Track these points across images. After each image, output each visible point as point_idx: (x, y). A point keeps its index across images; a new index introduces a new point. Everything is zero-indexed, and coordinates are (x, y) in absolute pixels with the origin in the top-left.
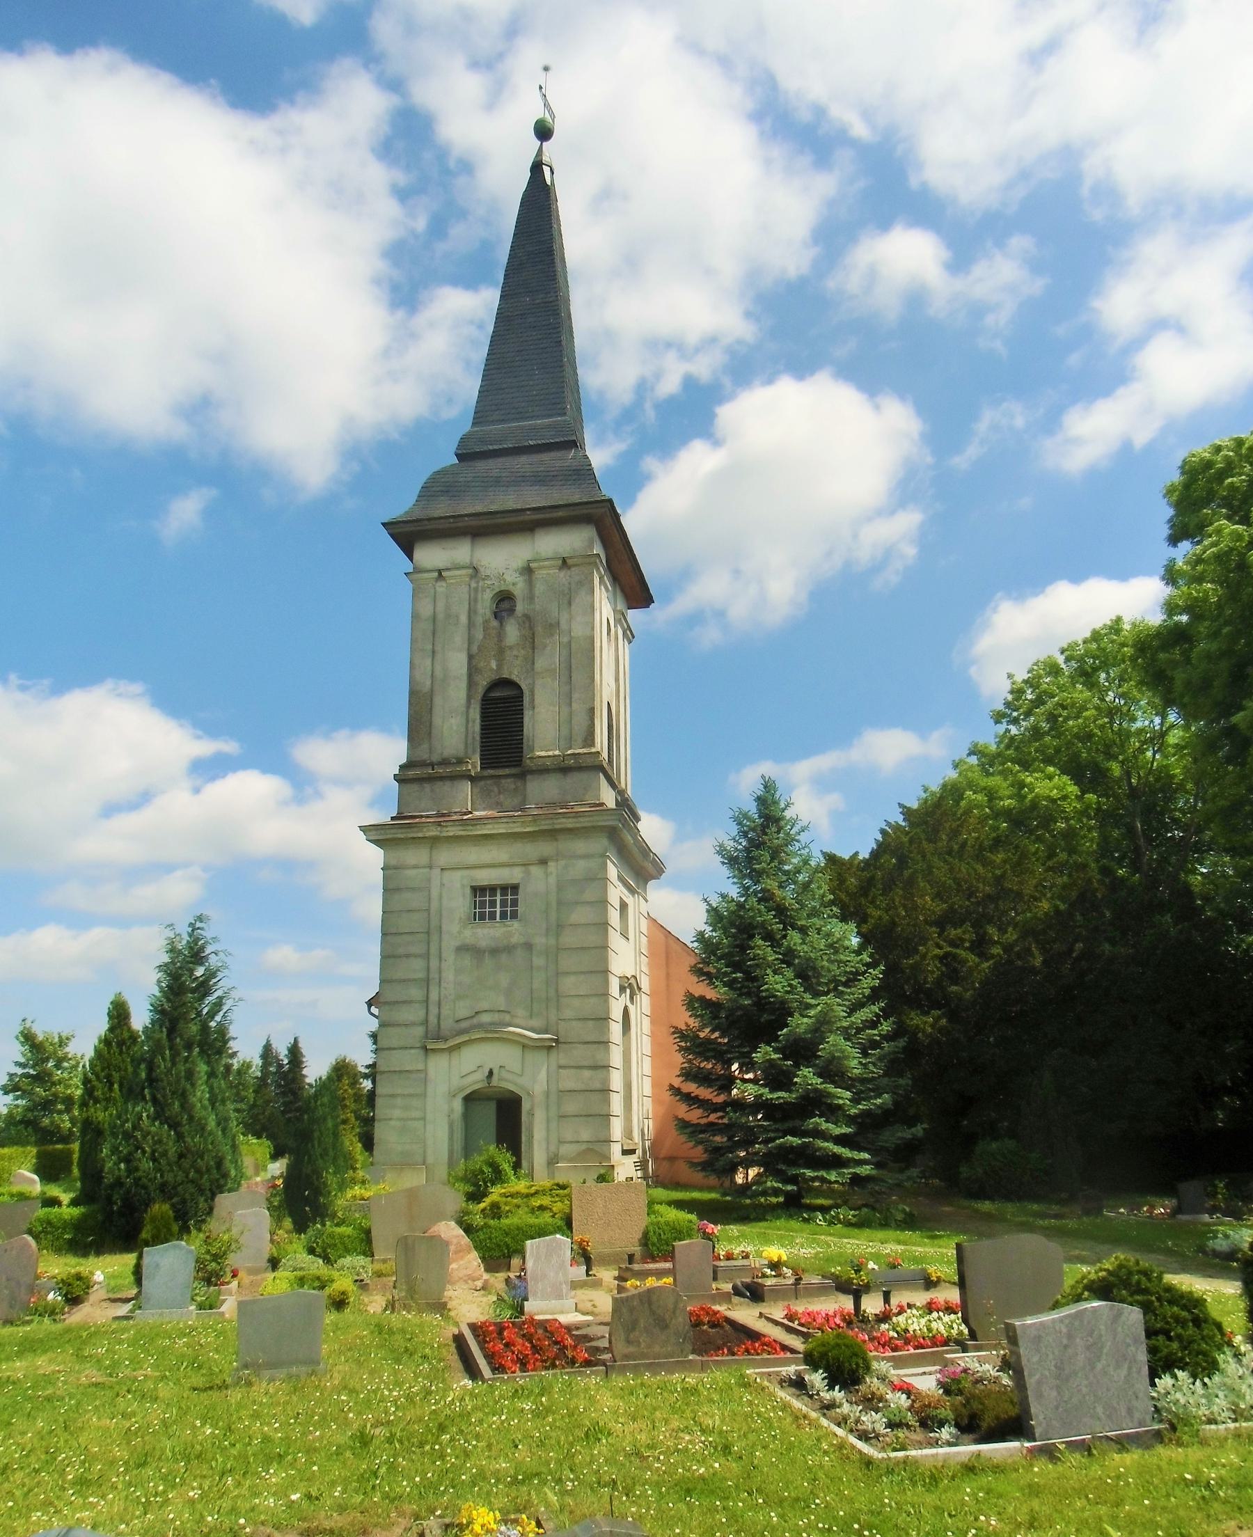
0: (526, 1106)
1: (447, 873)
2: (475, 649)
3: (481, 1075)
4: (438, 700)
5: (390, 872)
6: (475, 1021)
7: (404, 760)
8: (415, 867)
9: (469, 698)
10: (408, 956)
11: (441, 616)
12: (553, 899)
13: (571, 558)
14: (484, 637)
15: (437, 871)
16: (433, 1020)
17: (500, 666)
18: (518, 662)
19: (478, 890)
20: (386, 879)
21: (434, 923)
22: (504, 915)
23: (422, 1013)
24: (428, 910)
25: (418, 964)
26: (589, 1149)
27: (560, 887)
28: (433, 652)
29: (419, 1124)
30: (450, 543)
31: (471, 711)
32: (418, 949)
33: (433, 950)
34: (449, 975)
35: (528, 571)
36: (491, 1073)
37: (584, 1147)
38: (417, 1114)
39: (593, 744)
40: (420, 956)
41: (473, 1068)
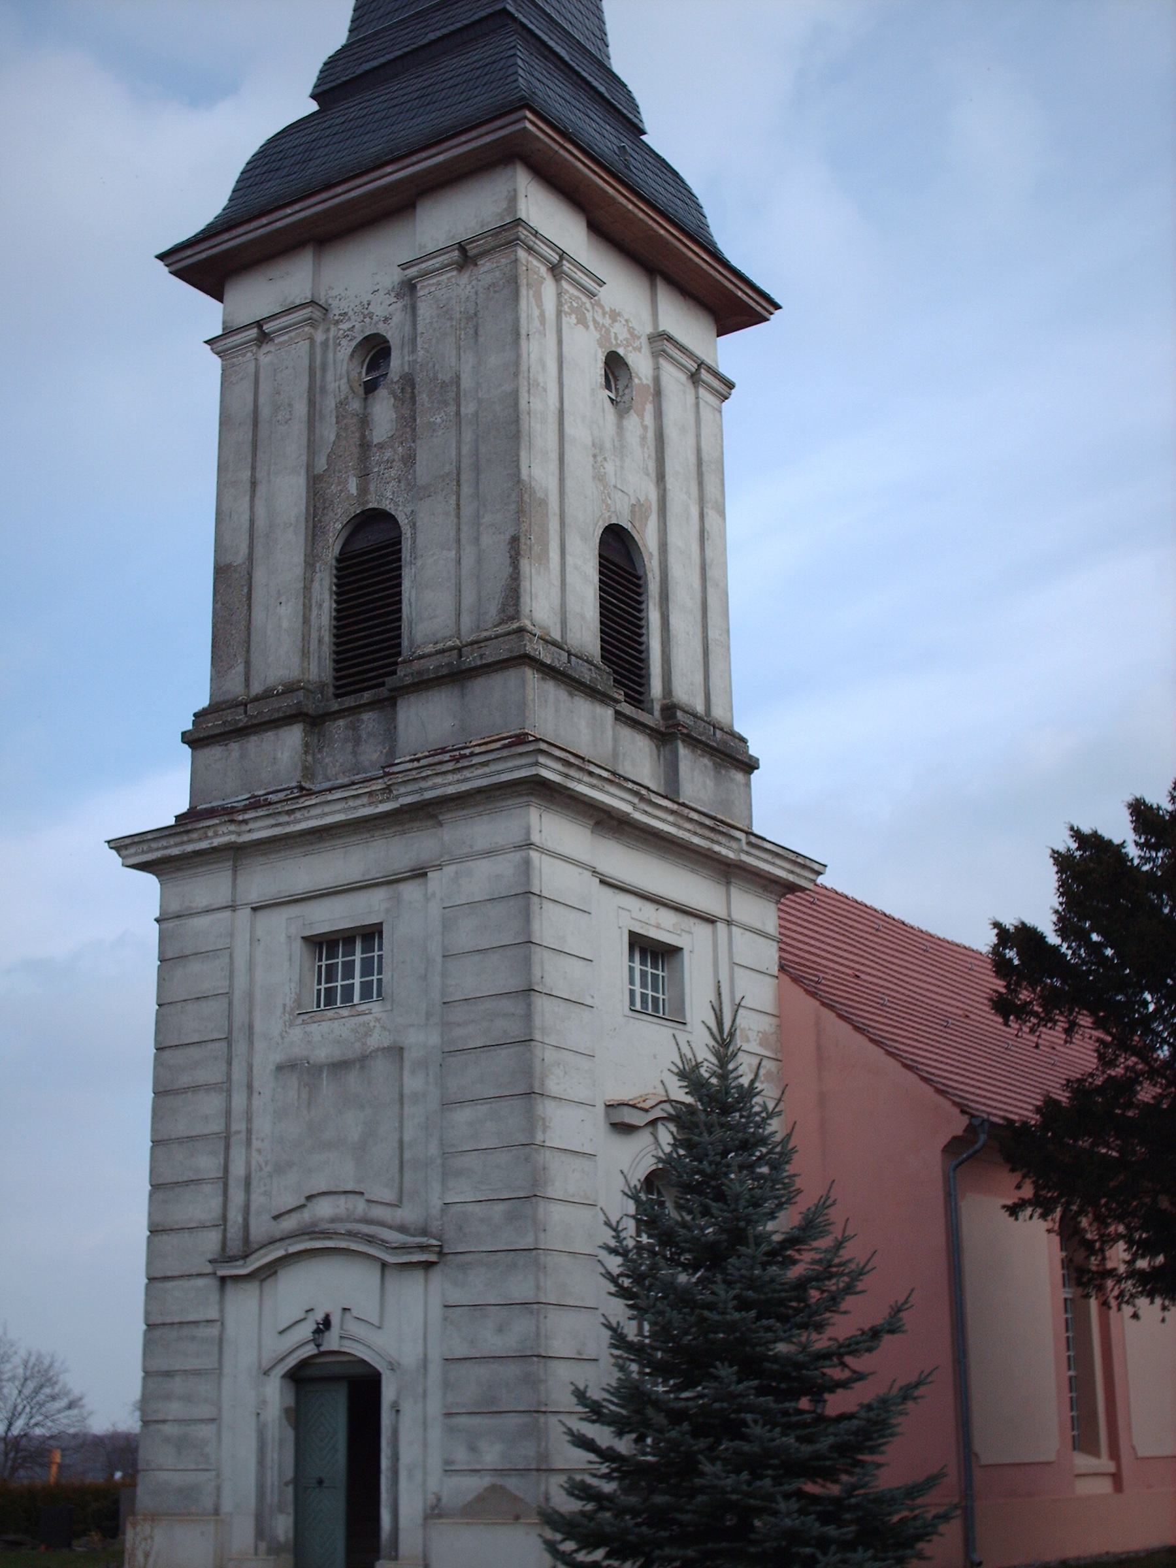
0: (388, 1394)
1: (261, 915)
2: (321, 464)
3: (305, 1331)
4: (259, 575)
5: (170, 925)
6: (306, 1216)
7: (204, 702)
8: (208, 911)
9: (310, 563)
10: (195, 1088)
11: (265, 412)
12: (435, 949)
13: (472, 240)
14: (338, 436)
15: (244, 914)
16: (235, 1217)
17: (363, 490)
18: (393, 472)
21: (239, 1018)
22: (366, 993)
23: (216, 1203)
24: (228, 995)
25: (212, 1104)
26: (493, 1489)
27: (447, 925)
28: (254, 484)
29: (206, 1431)
30: (278, 269)
31: (316, 585)
32: (212, 1074)
33: (238, 1074)
34: (263, 1125)
35: (409, 288)
36: (327, 1323)
37: (486, 1481)
38: (206, 1411)
39: (516, 616)
40: (208, 1088)
41: (300, 1315)
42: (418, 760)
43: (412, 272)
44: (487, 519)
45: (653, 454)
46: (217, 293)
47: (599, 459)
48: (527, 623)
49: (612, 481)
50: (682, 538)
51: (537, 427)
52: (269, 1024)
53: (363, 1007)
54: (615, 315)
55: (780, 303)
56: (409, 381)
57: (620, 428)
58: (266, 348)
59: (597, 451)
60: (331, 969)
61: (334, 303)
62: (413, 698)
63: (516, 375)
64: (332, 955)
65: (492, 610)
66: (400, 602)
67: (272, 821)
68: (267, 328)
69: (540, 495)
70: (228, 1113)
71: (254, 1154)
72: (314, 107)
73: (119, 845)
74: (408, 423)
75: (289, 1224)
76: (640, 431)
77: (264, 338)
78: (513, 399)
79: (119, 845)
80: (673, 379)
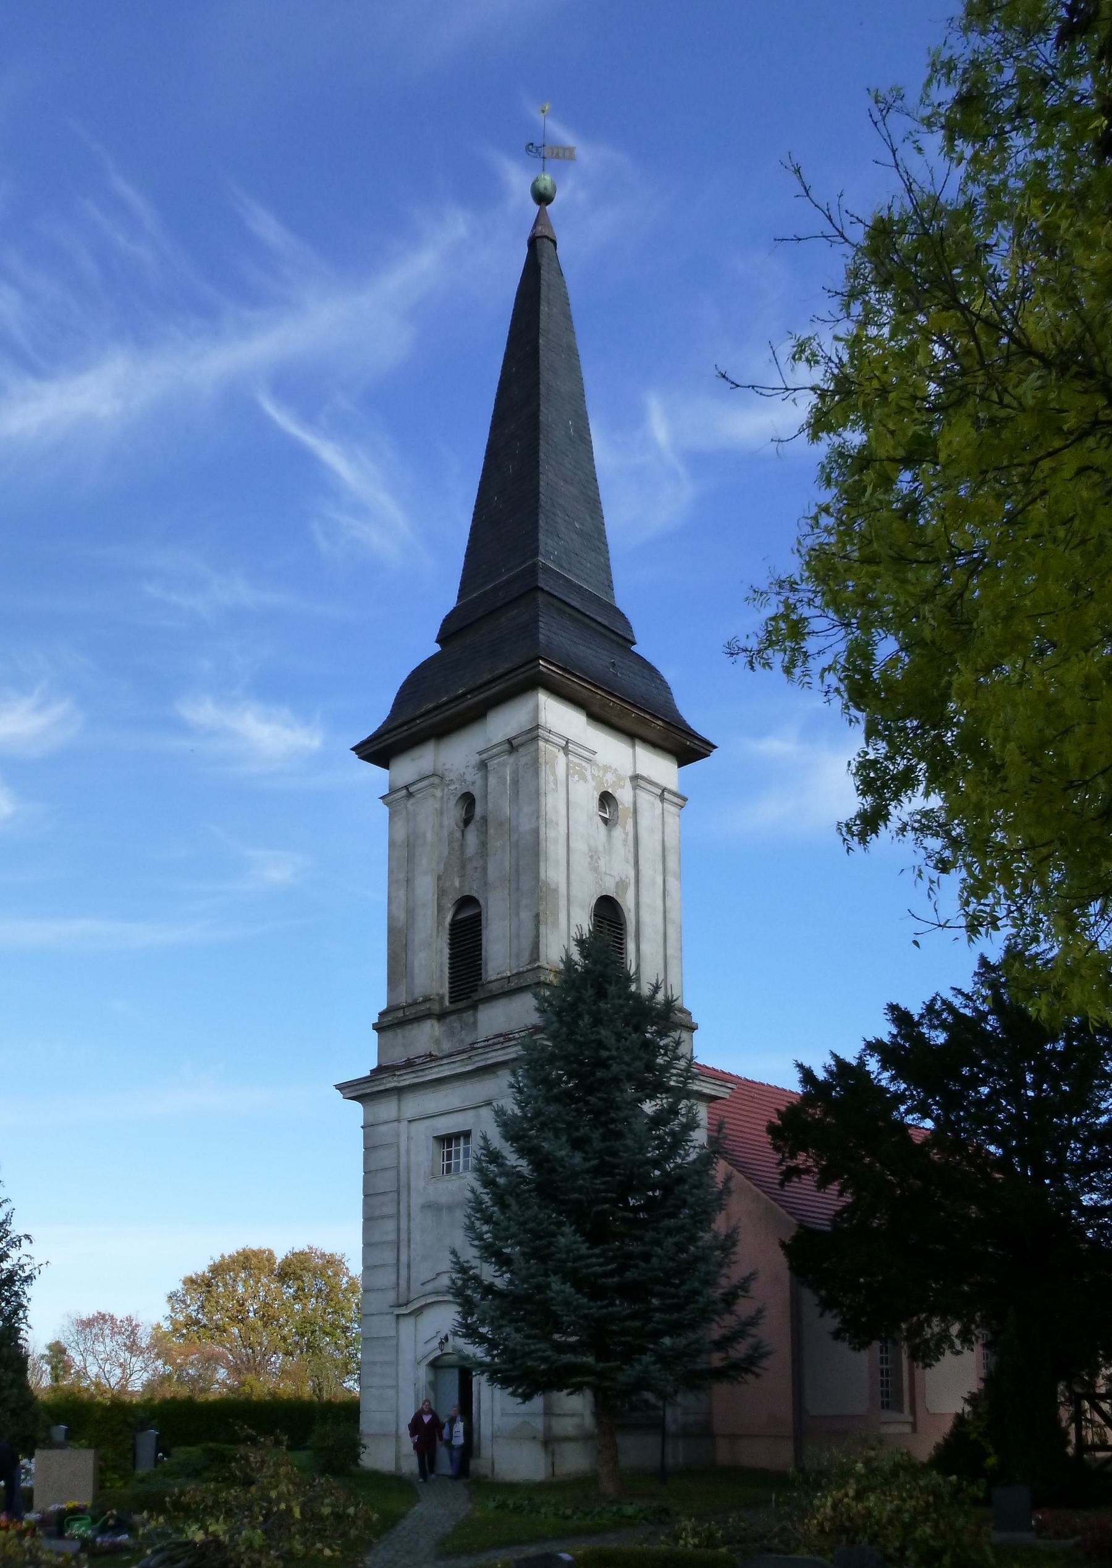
1: (415, 1125)
7: (383, 1006)
10: (383, 1217)
15: (404, 1124)
17: (462, 886)
19: (446, 1140)
20: (366, 1137)
23: (393, 1277)
24: (398, 1167)
30: (417, 752)
32: (390, 1209)
34: (416, 1236)
35: (483, 766)
36: (446, 1339)
39: (537, 959)
42: (488, 1040)
43: (485, 756)
44: (524, 902)
45: (632, 850)
46: (386, 765)
47: (595, 857)
48: (542, 963)
49: (603, 869)
50: (651, 897)
51: (551, 847)
52: (418, 1183)
53: (464, 1174)
54: (606, 768)
55: (716, 745)
56: (485, 819)
57: (609, 836)
58: (412, 800)
59: (593, 855)
60: (449, 1154)
61: (447, 774)
62: (487, 1005)
63: (538, 818)
64: (450, 1146)
65: (526, 956)
66: (481, 950)
67: (414, 1075)
68: (411, 789)
69: (553, 886)
70: (399, 1230)
71: (412, 1251)
72: (437, 648)
73: (341, 1087)
74: (483, 844)
75: (429, 1287)
76: (623, 836)
77: (410, 795)
78: (536, 831)
79: (341, 1087)
80: (646, 799)
